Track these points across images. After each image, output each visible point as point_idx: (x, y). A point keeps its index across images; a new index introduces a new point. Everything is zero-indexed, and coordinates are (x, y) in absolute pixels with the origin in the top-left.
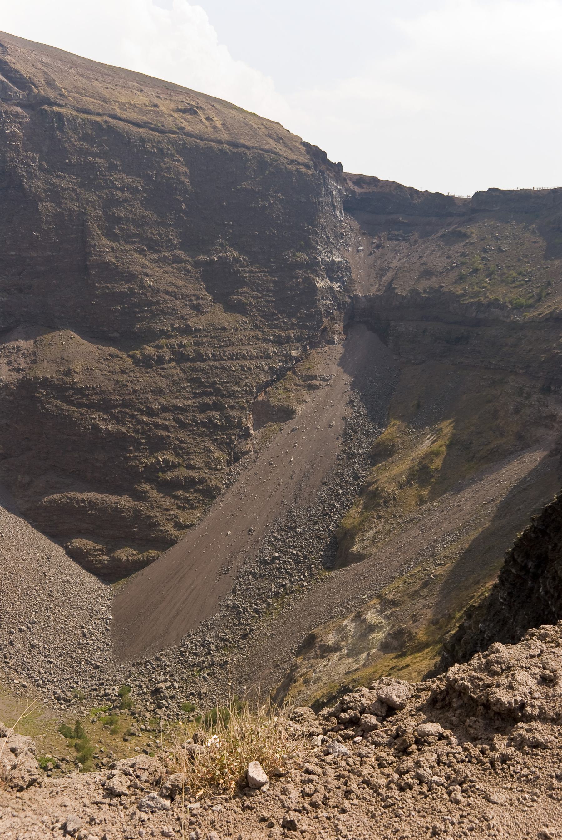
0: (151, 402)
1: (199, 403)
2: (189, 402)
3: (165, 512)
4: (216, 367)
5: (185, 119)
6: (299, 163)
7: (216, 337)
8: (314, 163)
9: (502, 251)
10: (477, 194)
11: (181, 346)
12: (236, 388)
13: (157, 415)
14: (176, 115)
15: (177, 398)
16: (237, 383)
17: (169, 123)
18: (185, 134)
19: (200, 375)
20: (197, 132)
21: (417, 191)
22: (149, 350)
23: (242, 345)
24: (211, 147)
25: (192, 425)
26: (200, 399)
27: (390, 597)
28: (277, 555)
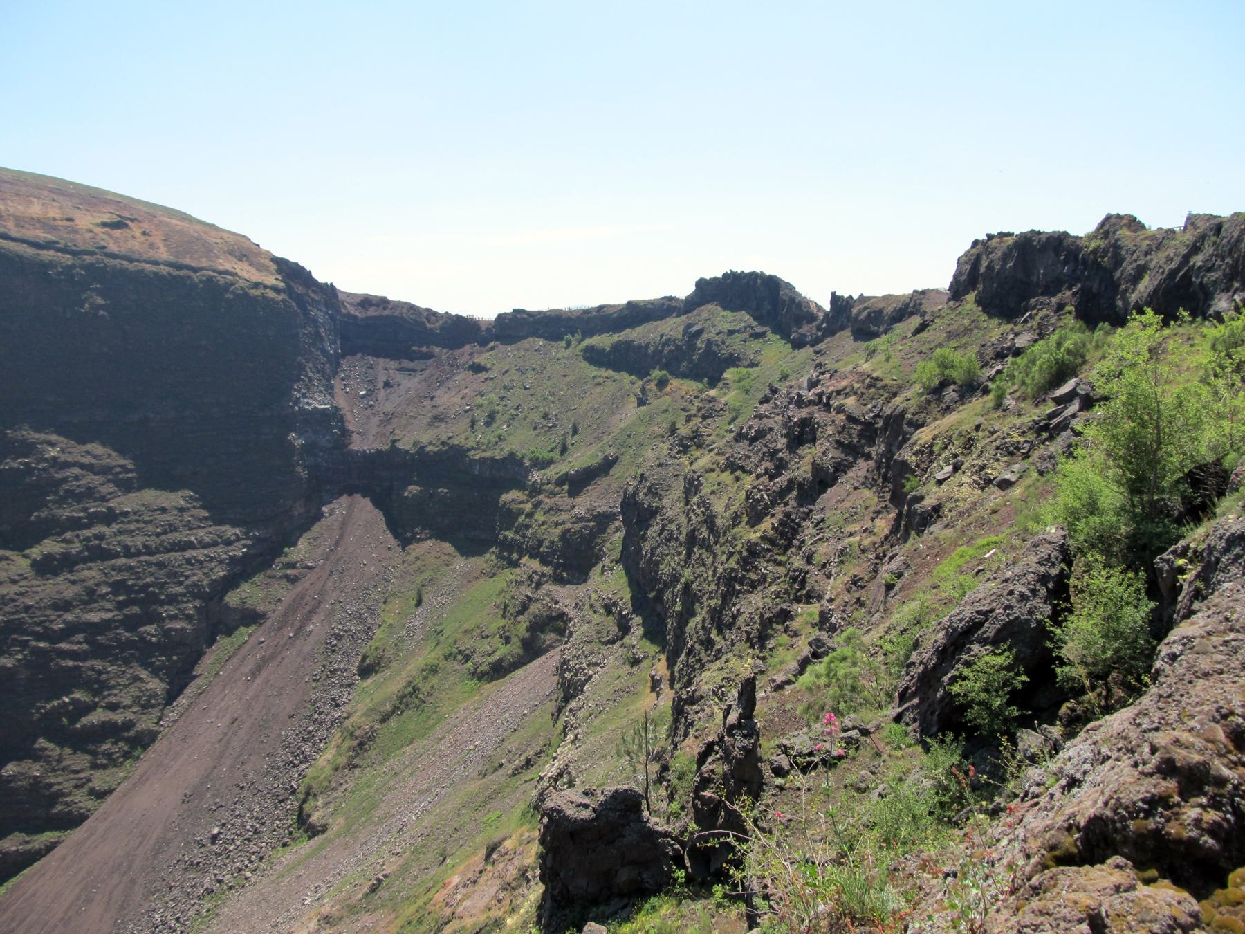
0: (52, 621)
1: (126, 615)
2: (109, 615)
3: (72, 776)
4: (150, 564)
5: (110, 236)
6: (265, 287)
7: (151, 521)
8: (288, 285)
9: (525, 388)
10: (501, 317)
11: (101, 537)
12: (179, 590)
13: (60, 641)
14: (98, 230)
15: (91, 611)
16: (181, 583)
17: (83, 242)
18: (106, 255)
19: (125, 575)
20: (123, 251)
21: (435, 314)
22: (51, 546)
23: (190, 529)
24: (143, 270)
25: (114, 648)
26: (126, 611)
27: (326, 910)
28: (216, 831)
